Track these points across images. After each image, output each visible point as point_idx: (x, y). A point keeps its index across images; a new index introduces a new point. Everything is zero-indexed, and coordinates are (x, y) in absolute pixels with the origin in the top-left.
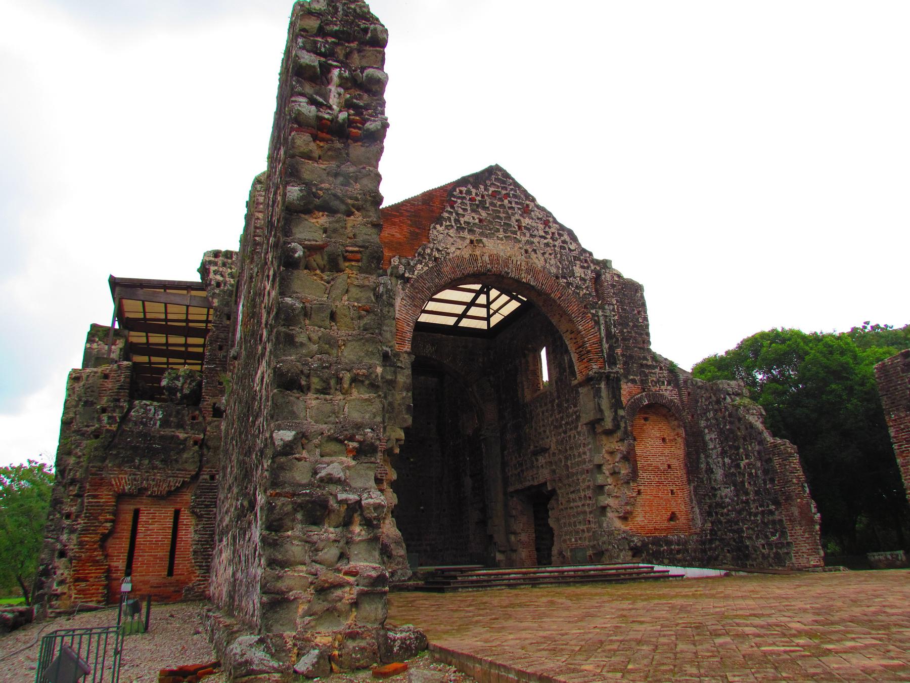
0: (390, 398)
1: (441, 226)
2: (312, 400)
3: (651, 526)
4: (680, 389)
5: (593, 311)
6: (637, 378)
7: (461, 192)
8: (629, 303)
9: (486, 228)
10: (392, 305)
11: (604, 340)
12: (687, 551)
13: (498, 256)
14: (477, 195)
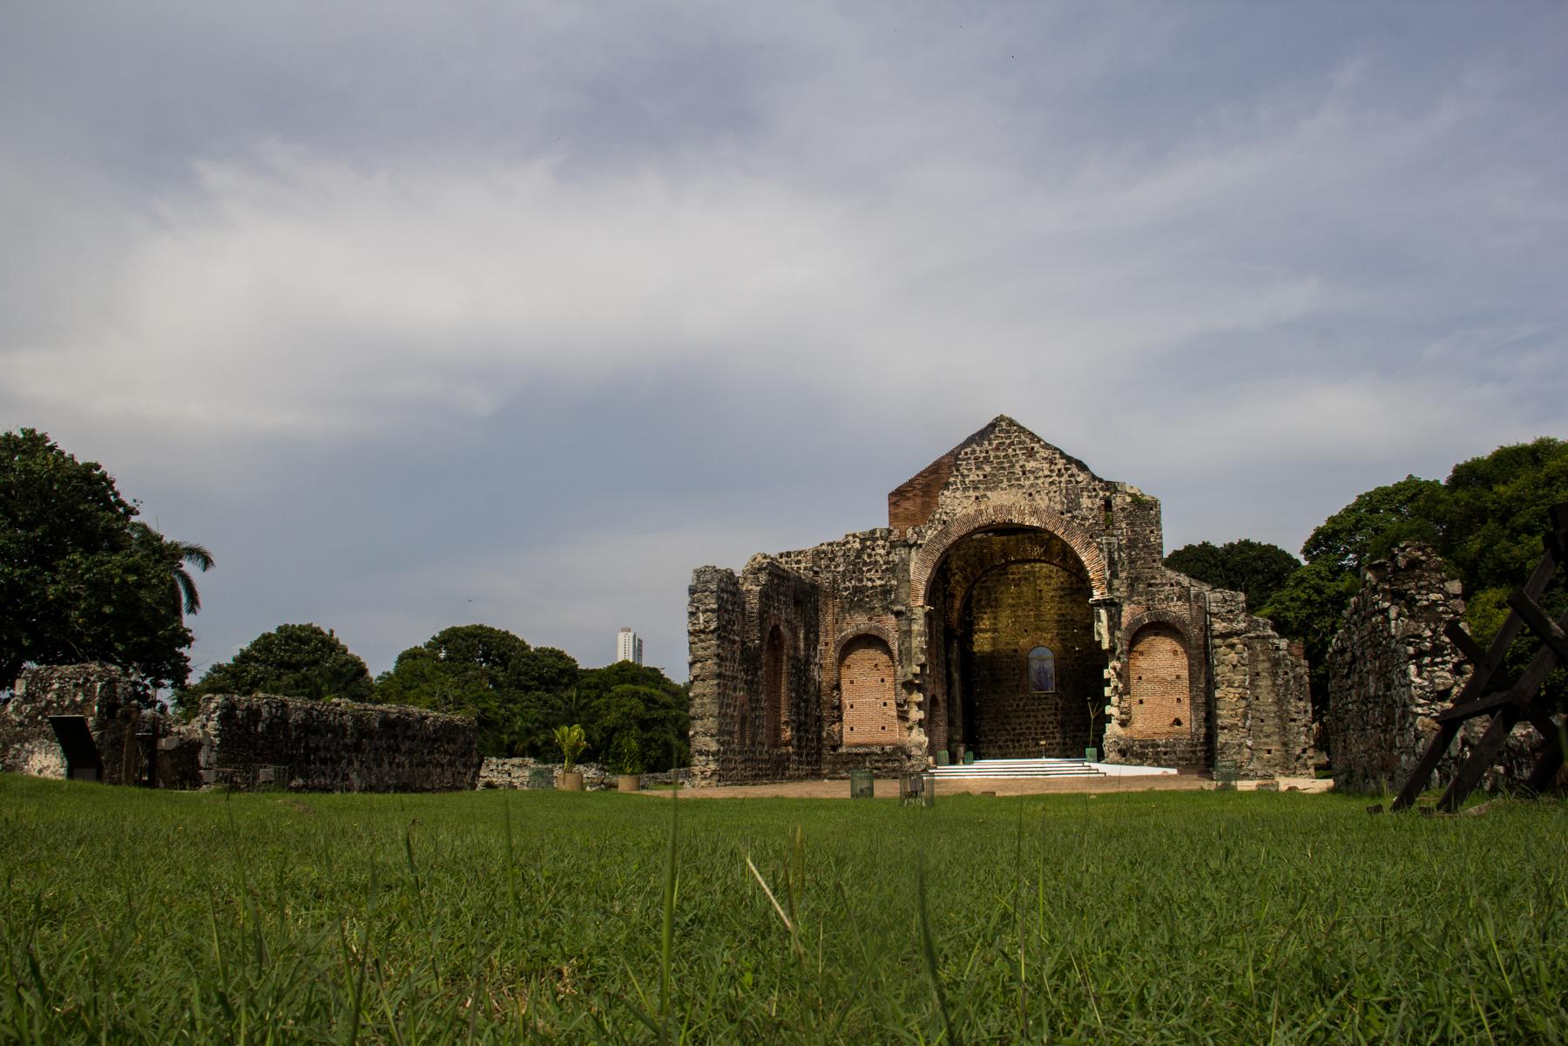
0: (907, 645)
1: (948, 490)
2: (699, 722)
3: (1149, 732)
4: (1190, 605)
5: (1099, 540)
6: (1142, 599)
7: (966, 453)
8: (1141, 524)
9: (991, 482)
10: (907, 571)
11: (1106, 567)
12: (1175, 753)
13: (1002, 506)
14: (981, 452)
